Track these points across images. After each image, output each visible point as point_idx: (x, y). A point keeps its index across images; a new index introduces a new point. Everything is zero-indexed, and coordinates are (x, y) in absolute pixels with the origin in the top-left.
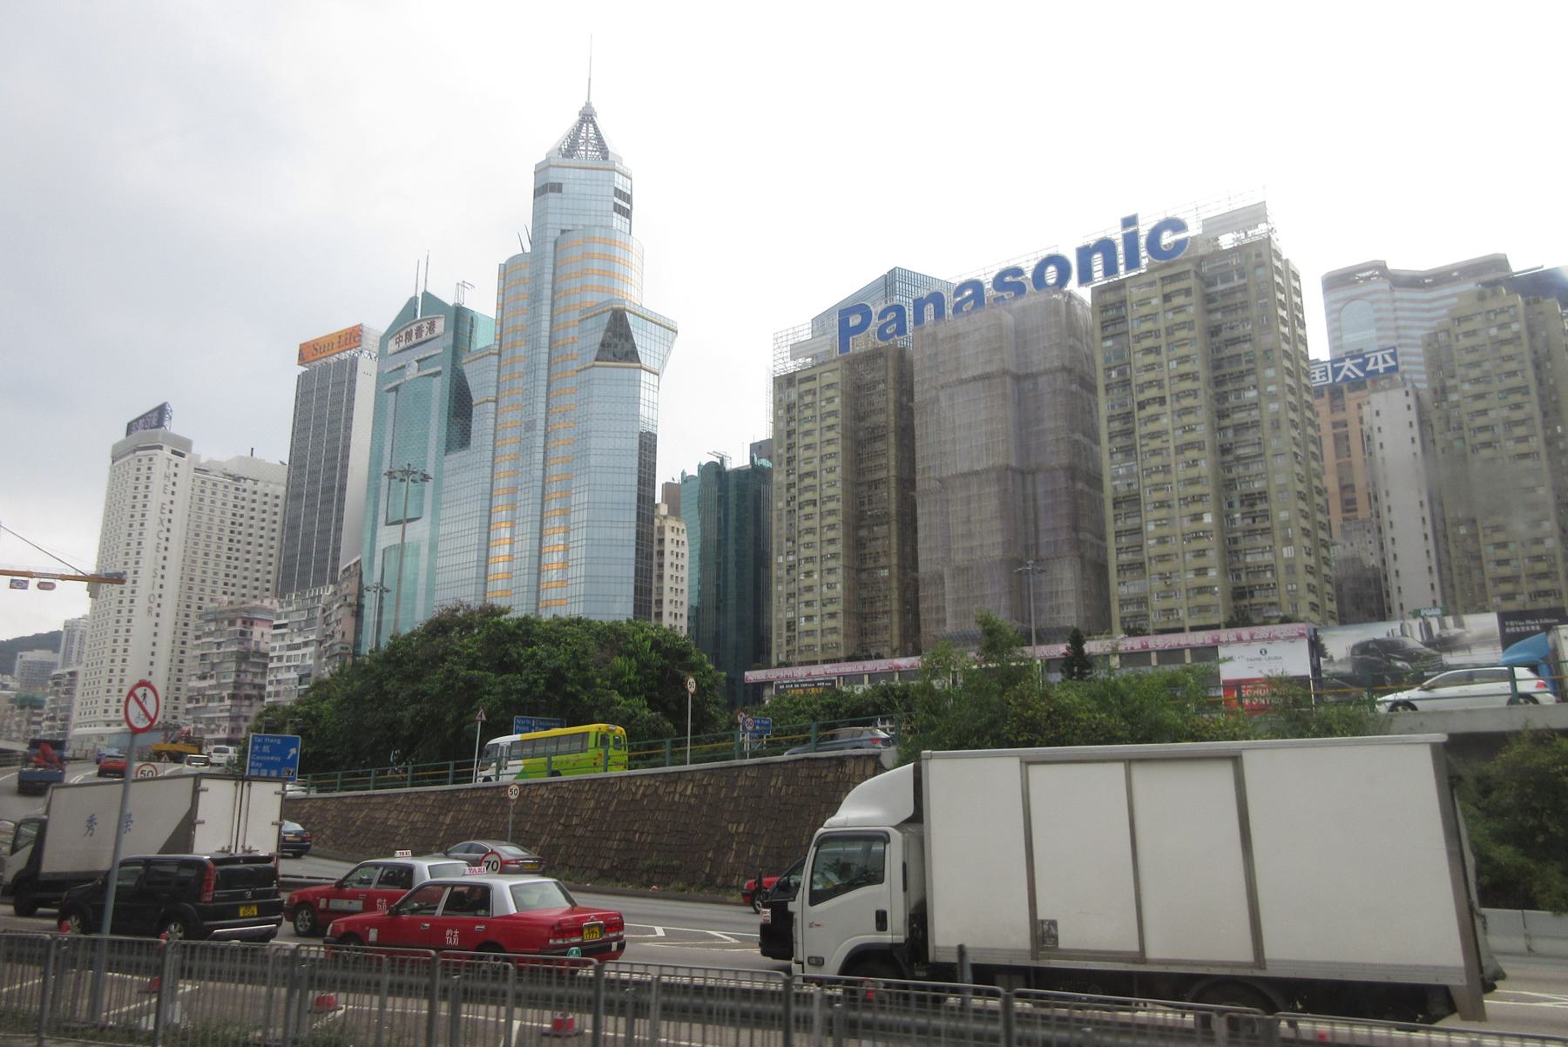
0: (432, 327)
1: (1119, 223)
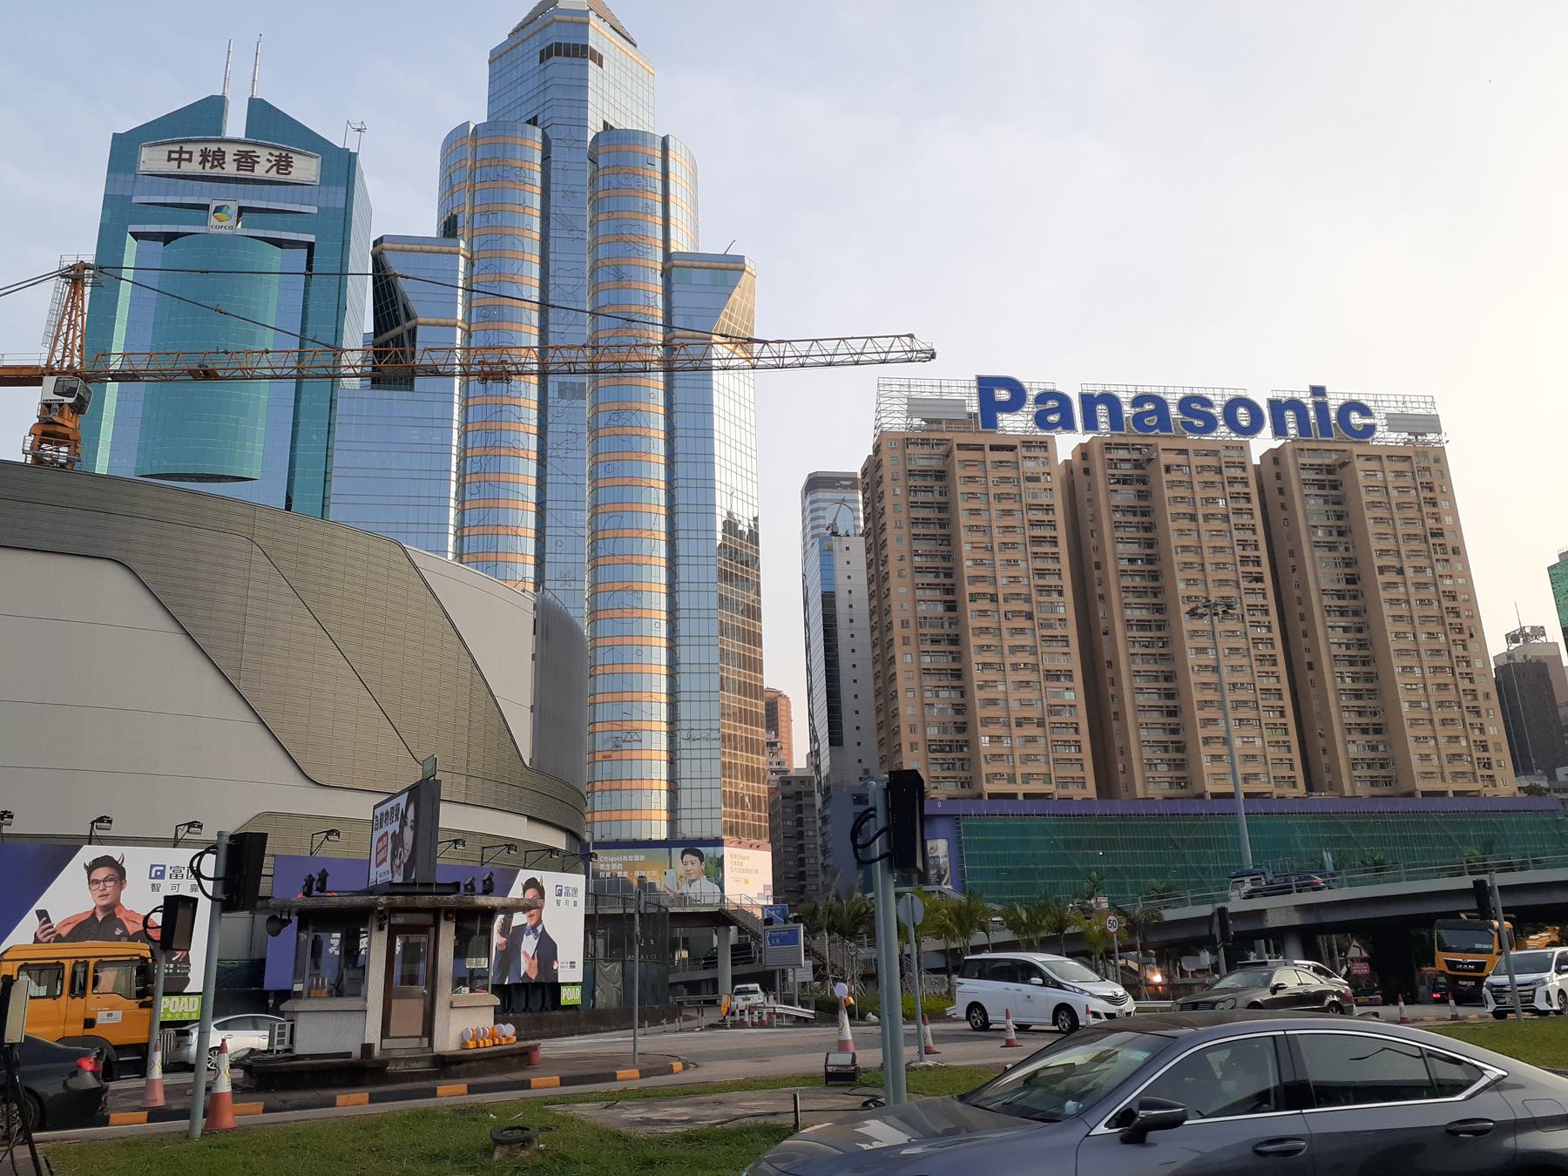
0: (283, 163)
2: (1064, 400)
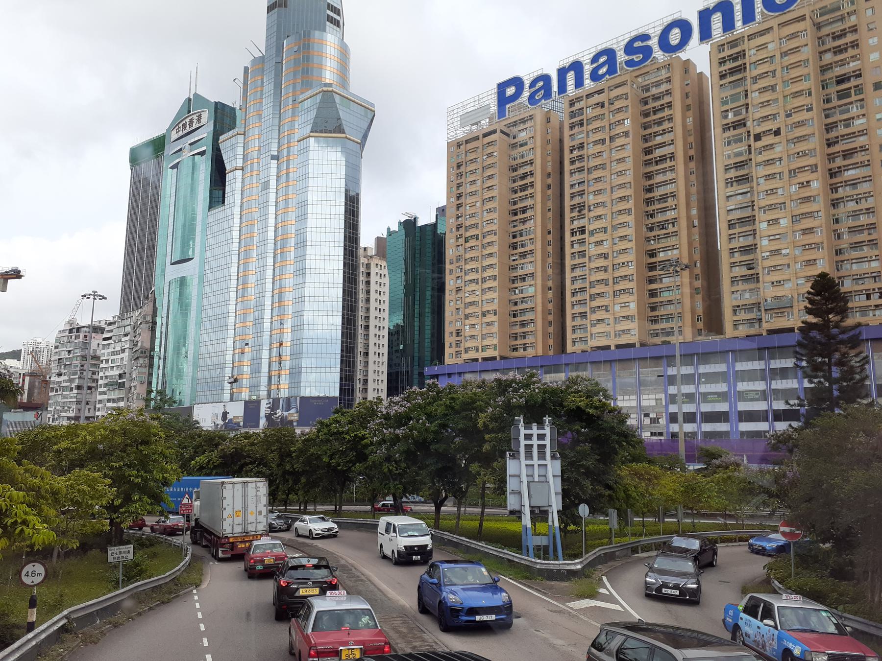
2: (546, 78)
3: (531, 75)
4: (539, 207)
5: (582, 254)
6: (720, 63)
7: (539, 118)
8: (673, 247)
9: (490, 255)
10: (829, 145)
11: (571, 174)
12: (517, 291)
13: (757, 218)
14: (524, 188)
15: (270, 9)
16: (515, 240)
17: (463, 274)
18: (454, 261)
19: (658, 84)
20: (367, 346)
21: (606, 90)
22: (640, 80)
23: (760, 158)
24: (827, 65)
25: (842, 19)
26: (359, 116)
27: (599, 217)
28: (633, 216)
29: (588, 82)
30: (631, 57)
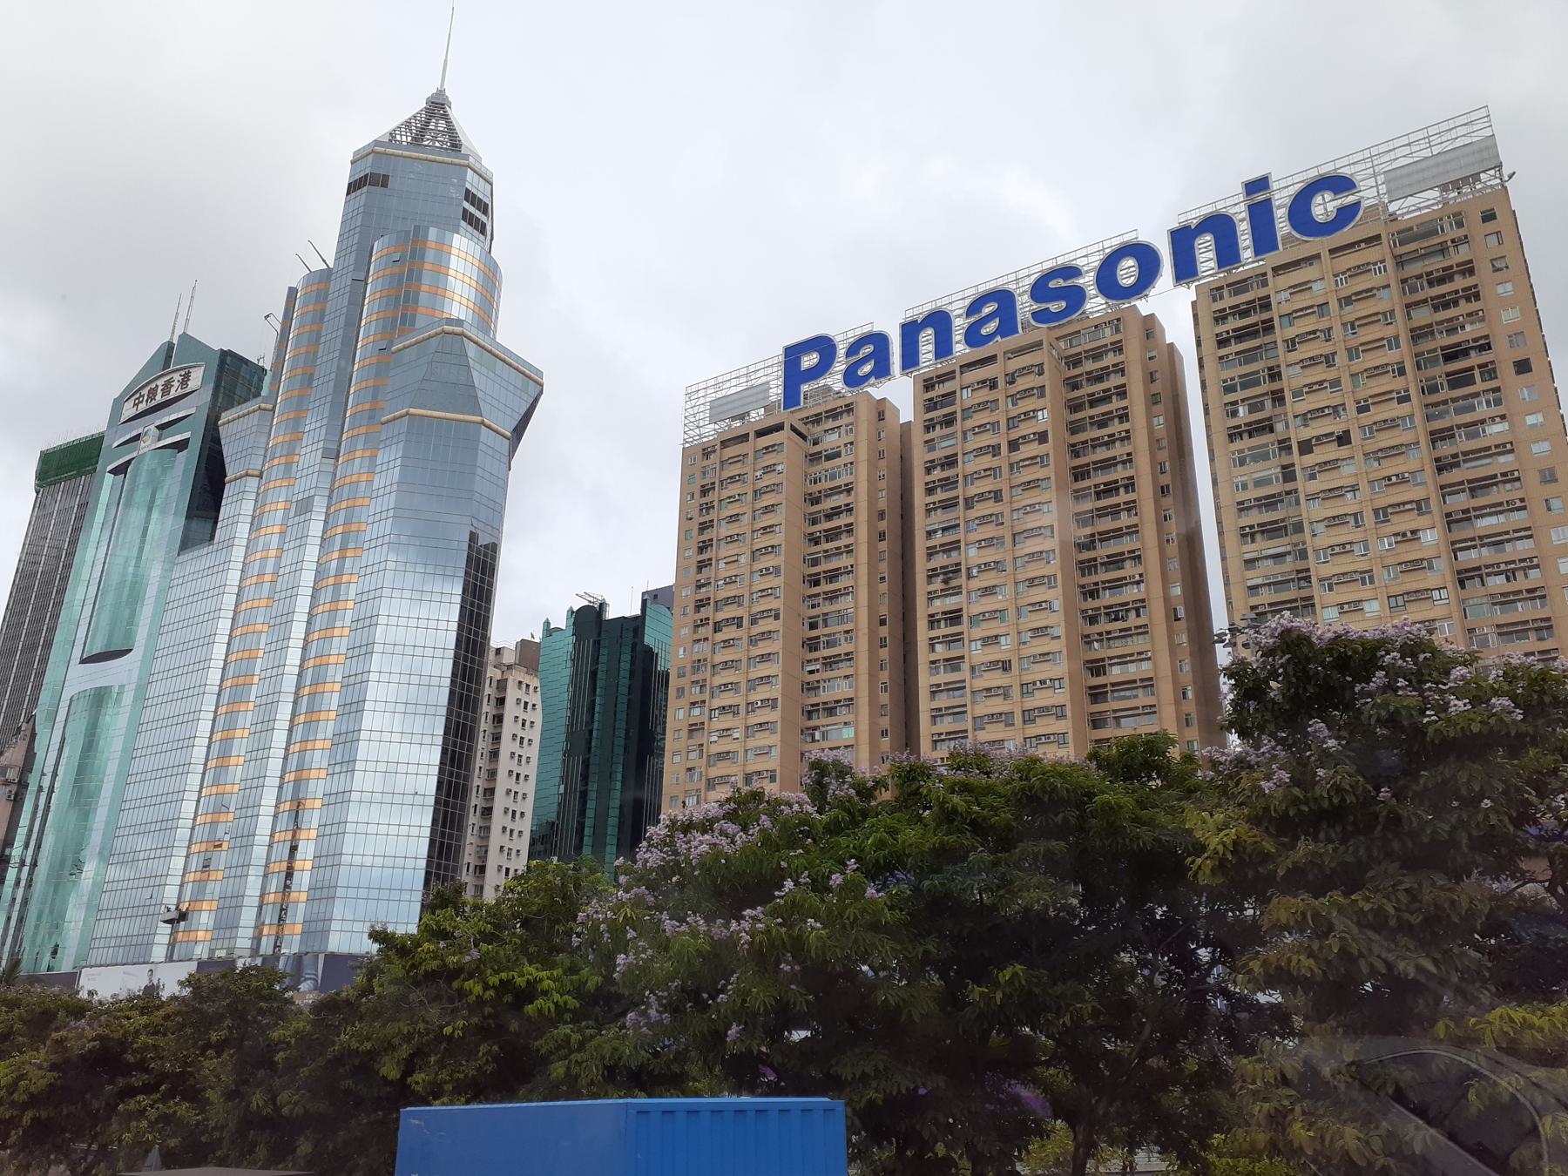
1: (1240, 189)
2: (878, 341)
3: (850, 334)
4: (863, 571)
5: (953, 663)
6: (1216, 320)
7: (864, 413)
8: (1141, 657)
9: (765, 658)
10: (1440, 470)
11: (928, 511)
12: (818, 735)
13: (1316, 600)
14: (832, 535)
15: (353, 187)
16: (814, 633)
17: (706, 696)
18: (688, 669)
19: (1097, 355)
20: (483, 852)
21: (1000, 359)
22: (1062, 344)
23: (1315, 486)
24: (1421, 328)
25: (1442, 250)
26: (511, 388)
27: (988, 591)
28: (1059, 589)
29: (960, 348)
30: (1044, 306)
